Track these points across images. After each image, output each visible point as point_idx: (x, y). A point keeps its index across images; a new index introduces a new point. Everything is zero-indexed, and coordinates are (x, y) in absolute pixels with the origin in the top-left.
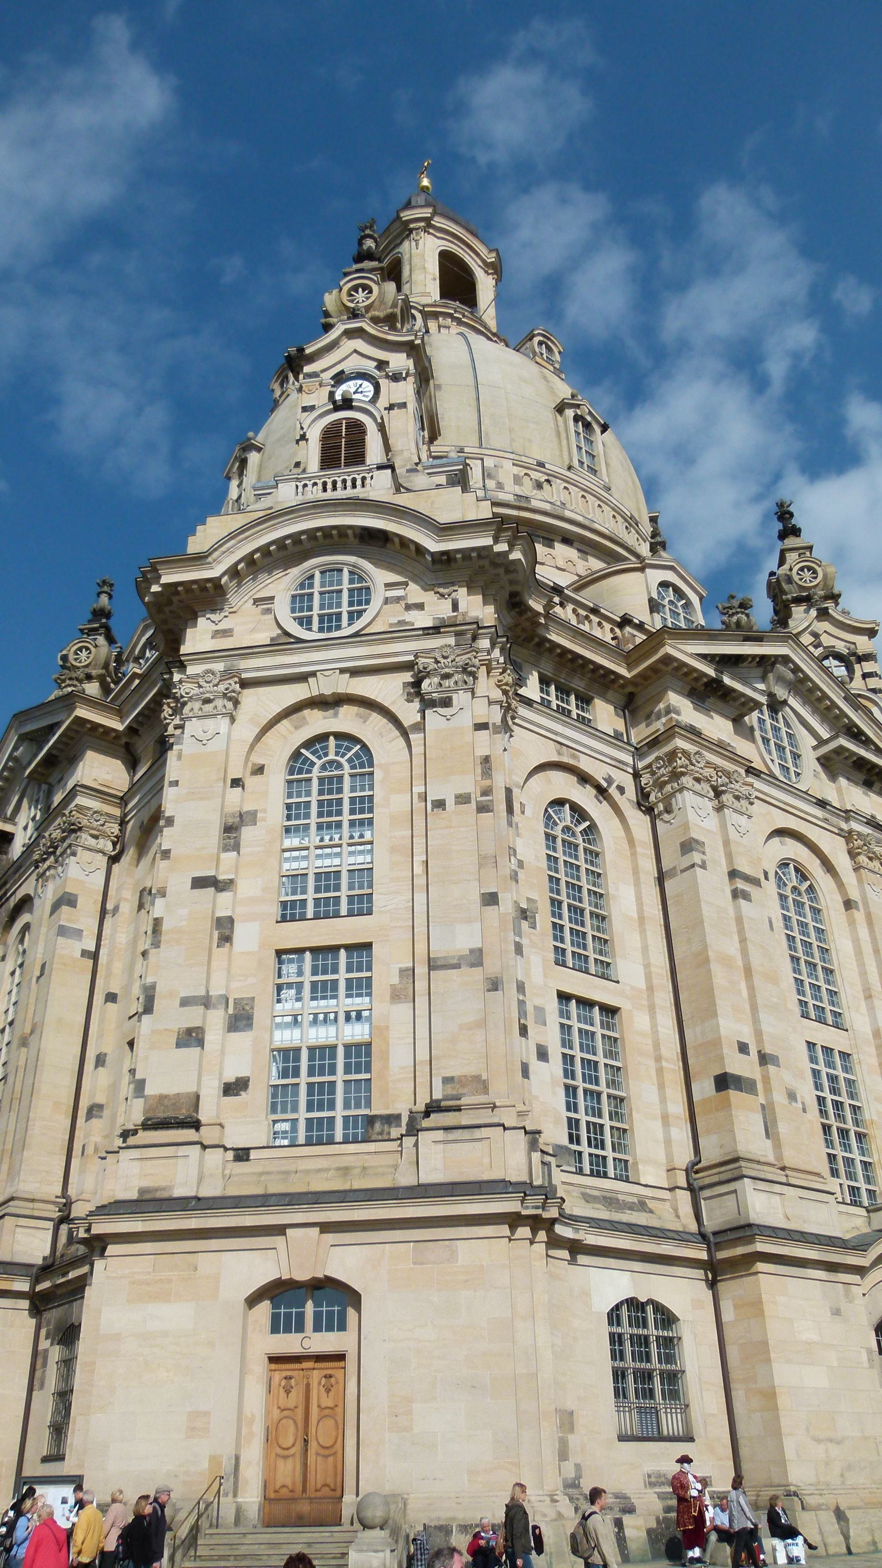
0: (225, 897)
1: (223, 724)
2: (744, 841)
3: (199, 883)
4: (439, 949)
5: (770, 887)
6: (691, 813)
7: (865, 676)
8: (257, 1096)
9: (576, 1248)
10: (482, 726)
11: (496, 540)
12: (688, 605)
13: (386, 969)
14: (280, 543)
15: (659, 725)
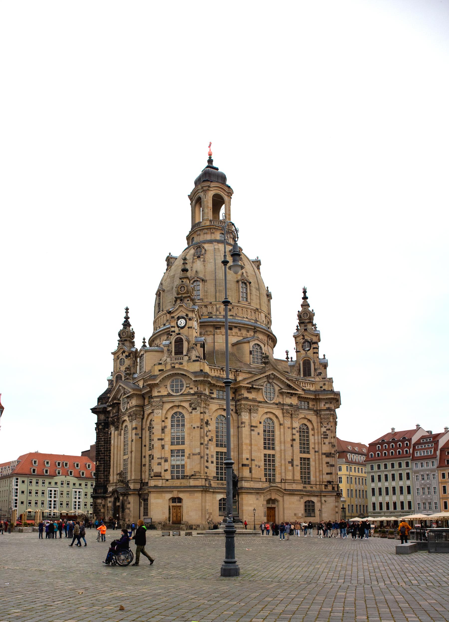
0: (163, 441)
1: (160, 411)
2: (255, 419)
3: (159, 439)
4: (194, 452)
5: (262, 425)
6: (243, 417)
7: (314, 348)
8: (169, 472)
9: (213, 492)
10: (201, 413)
11: (204, 377)
12: (261, 348)
13: (186, 454)
14: (168, 375)
15: (240, 397)
